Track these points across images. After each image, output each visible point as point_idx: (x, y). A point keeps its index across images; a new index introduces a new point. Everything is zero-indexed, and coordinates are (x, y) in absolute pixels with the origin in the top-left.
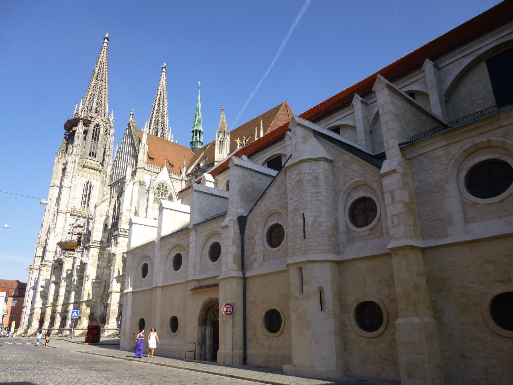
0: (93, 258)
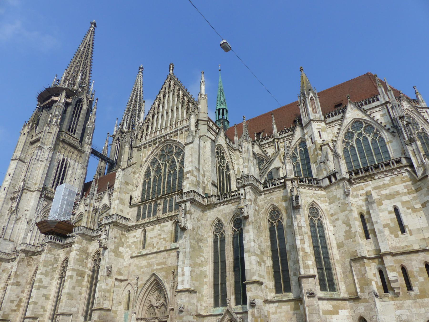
0: (115, 242)
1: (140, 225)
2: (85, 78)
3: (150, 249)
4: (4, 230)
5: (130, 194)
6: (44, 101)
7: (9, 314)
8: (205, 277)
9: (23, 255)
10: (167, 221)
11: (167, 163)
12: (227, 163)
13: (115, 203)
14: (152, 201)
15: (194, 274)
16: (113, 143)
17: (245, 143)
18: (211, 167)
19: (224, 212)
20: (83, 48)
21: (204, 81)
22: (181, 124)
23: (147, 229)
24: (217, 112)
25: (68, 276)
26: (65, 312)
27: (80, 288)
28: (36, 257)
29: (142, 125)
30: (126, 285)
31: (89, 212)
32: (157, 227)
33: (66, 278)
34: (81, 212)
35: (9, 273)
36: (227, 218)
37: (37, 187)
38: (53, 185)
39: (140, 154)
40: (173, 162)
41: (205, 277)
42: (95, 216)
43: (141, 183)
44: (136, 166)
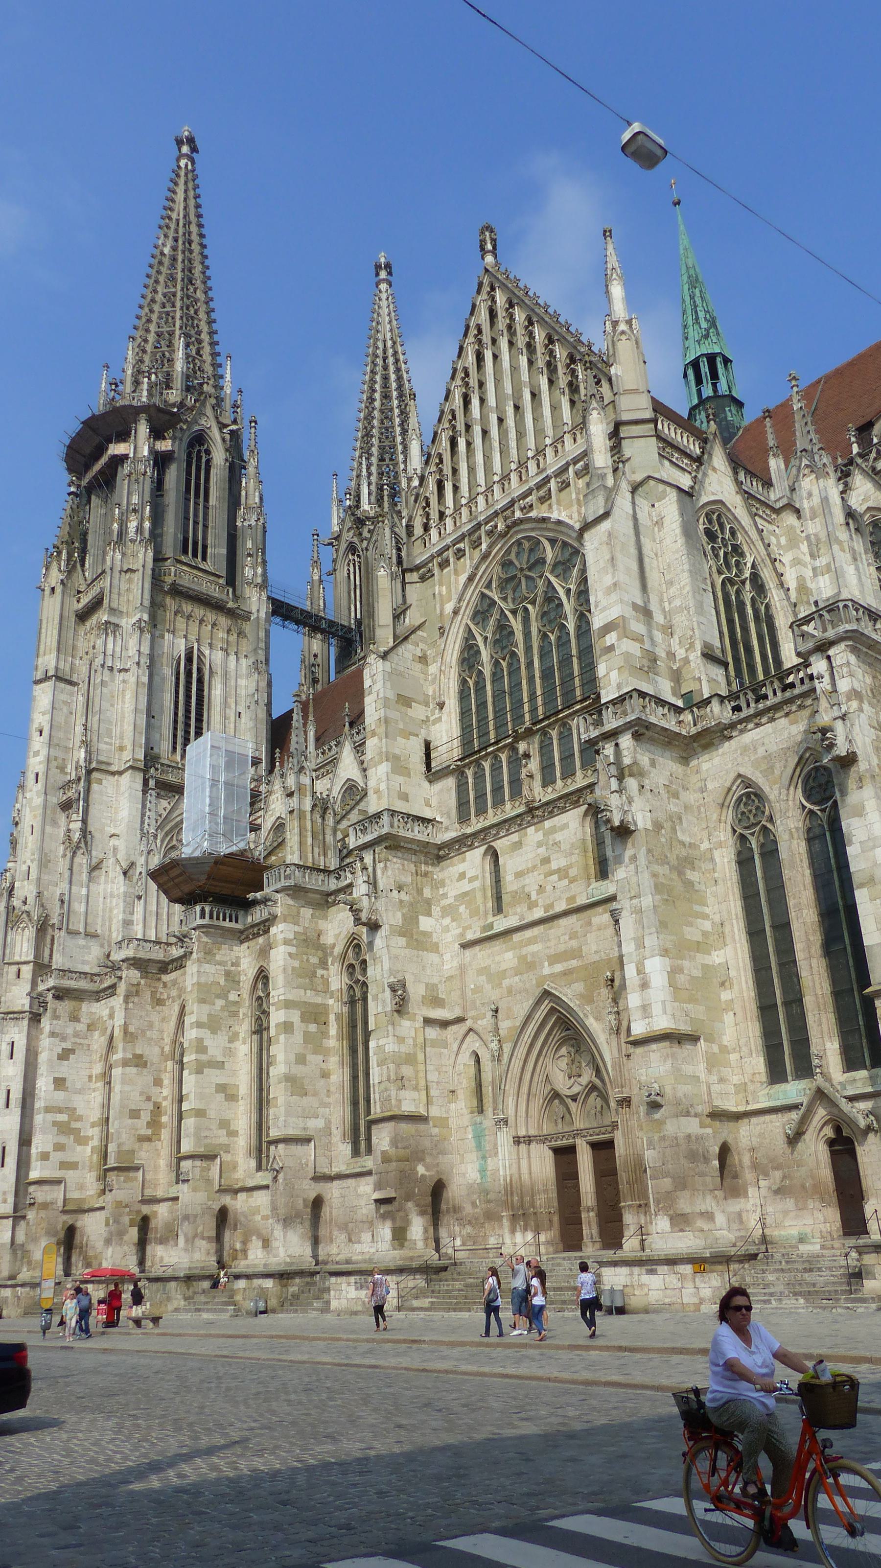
0: (401, 901)
1: (474, 835)
2: (198, 352)
3: (519, 910)
4: (66, 905)
5: (423, 734)
6: (87, 467)
7: (133, 1152)
8: (723, 984)
9: (132, 975)
10: (564, 810)
11: (529, 607)
12: (754, 566)
13: (379, 773)
14: (498, 750)
15: (682, 979)
16: (338, 567)
17: (807, 479)
18: (690, 594)
19: (761, 751)
20: (170, 243)
21: (616, 265)
22: (556, 452)
23: (498, 845)
24: (690, 372)
25: (277, 1025)
26: (291, 1132)
27: (321, 1058)
28: (173, 976)
29: (421, 484)
30: (460, 1038)
31: (301, 816)
32: (533, 834)
33: (272, 1032)
34: (279, 818)
35: (109, 1032)
36: (777, 772)
37: (127, 755)
38: (175, 743)
39: (430, 592)
40: (551, 597)
41: (723, 984)
42: (323, 824)
43: (452, 690)
44: (425, 635)
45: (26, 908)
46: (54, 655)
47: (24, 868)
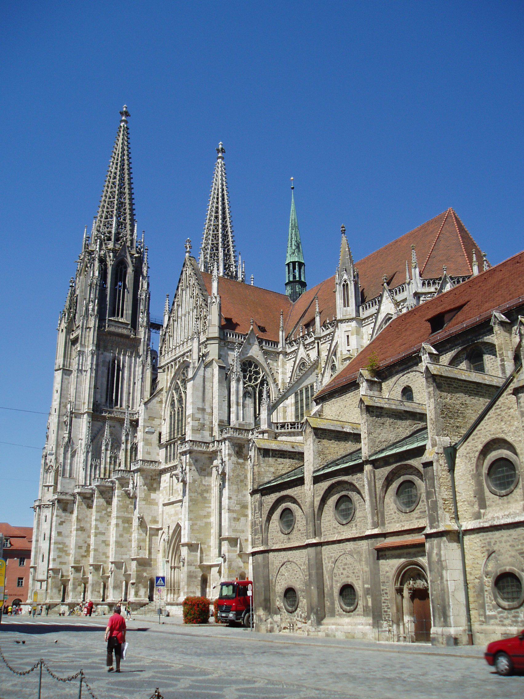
1: (168, 468)
7: (79, 561)
15: (196, 527)
45: (51, 464)
46: (62, 359)
47: (51, 447)
